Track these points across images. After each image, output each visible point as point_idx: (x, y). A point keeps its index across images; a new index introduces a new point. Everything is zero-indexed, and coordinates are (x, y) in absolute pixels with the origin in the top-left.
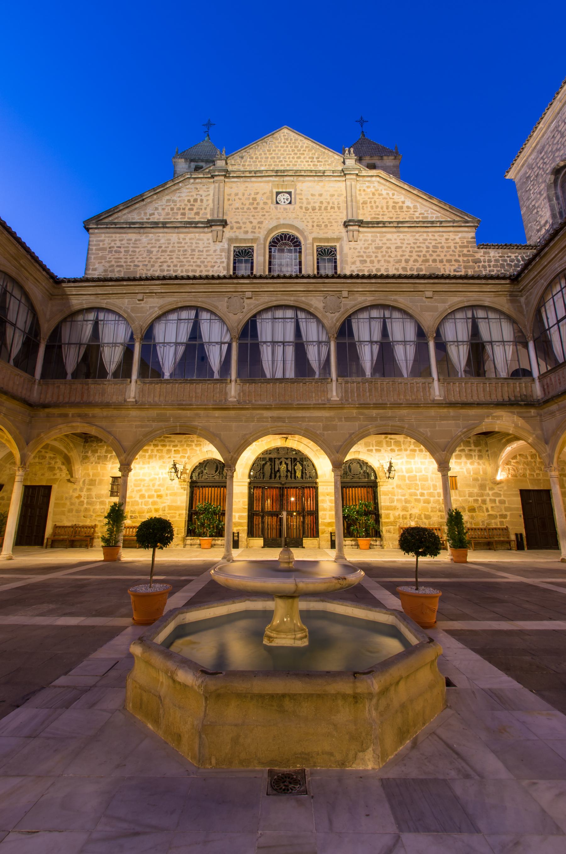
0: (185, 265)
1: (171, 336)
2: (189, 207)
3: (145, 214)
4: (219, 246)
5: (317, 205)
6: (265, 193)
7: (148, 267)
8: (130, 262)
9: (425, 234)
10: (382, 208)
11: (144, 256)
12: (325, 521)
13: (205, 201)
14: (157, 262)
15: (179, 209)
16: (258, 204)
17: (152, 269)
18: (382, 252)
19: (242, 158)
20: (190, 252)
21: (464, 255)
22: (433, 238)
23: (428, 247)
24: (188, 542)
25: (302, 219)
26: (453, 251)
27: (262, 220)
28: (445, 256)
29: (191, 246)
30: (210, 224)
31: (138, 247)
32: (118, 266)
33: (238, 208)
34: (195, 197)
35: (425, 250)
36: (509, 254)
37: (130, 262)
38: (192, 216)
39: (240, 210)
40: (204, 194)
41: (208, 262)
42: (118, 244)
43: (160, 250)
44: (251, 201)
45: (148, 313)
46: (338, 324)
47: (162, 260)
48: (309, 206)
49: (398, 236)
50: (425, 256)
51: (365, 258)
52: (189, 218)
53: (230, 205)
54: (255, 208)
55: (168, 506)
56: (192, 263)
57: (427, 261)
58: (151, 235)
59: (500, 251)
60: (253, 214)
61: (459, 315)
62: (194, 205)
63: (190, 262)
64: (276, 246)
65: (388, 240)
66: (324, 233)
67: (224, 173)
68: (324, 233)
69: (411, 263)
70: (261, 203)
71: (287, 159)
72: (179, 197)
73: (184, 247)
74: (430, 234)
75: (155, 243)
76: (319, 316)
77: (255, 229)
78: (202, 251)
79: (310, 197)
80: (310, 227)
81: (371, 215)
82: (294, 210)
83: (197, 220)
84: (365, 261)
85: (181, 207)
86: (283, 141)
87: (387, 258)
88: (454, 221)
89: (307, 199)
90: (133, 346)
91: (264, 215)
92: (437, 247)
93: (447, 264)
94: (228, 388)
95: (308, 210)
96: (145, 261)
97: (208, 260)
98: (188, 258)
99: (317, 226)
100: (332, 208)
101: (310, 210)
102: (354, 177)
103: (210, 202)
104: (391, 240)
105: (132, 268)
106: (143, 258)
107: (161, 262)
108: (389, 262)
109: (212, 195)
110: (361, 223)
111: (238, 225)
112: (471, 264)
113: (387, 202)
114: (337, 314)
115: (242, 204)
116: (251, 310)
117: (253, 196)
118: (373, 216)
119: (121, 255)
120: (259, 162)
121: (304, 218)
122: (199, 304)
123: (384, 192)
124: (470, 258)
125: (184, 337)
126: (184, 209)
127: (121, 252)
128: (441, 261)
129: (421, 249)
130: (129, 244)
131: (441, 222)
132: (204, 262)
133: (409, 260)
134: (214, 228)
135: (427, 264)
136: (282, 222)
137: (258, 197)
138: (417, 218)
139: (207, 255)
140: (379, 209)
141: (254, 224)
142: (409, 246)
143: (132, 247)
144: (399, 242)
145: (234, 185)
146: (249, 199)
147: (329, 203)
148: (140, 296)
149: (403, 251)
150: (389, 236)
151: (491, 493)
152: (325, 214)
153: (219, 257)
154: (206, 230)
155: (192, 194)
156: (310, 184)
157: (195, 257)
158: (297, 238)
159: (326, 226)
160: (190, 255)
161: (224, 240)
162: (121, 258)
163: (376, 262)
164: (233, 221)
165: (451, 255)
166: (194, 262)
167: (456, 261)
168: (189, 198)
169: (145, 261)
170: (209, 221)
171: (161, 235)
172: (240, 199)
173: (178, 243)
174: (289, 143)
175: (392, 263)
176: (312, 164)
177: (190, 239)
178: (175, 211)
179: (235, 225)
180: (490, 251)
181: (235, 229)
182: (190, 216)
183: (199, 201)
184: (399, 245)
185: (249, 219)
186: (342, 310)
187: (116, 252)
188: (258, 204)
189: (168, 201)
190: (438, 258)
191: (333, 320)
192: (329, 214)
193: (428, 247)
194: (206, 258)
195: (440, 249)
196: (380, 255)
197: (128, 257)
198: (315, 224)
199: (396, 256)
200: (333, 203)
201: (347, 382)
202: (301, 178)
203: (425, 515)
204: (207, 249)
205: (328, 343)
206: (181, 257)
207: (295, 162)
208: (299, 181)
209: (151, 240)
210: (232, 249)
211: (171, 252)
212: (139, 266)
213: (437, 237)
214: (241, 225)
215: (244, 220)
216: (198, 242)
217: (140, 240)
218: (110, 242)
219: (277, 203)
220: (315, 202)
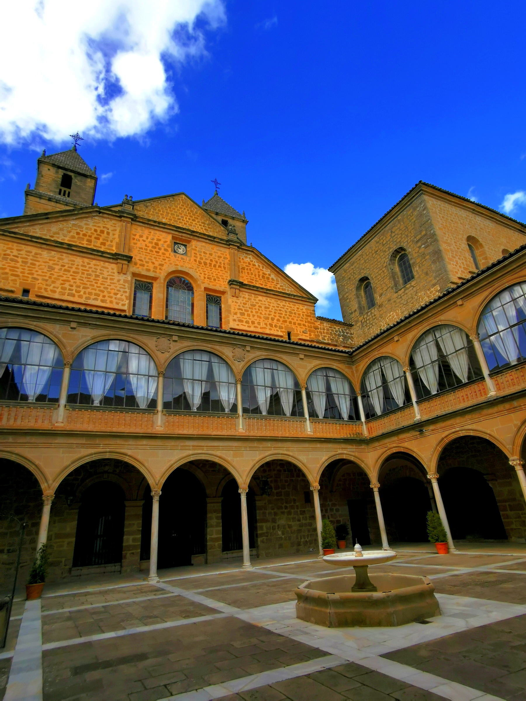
0: (89, 288)
2: (95, 236)
3: (49, 230)
4: (122, 277)
5: (208, 262)
6: (166, 242)
7: (49, 283)
8: (28, 274)
9: (284, 302)
10: (255, 276)
11: (45, 271)
12: (212, 537)
13: (111, 234)
14: (59, 279)
15: (85, 235)
16: (160, 249)
17: (53, 285)
18: (255, 309)
19: (147, 207)
20: (93, 277)
21: (309, 322)
22: (289, 305)
23: (286, 312)
24: (73, 573)
25: (196, 269)
26: (302, 318)
27: (162, 263)
28: (297, 320)
29: (96, 272)
30: (116, 257)
31: (39, 261)
32: (12, 275)
33: (142, 248)
34: (102, 229)
35: (284, 313)
36: (335, 327)
37: (28, 274)
38: (98, 244)
39: (144, 250)
40: (111, 228)
41: (111, 289)
42: (15, 253)
43: (63, 268)
44: (154, 245)
45: (80, 341)
46: (243, 370)
47: (64, 278)
48: (202, 261)
49: (267, 299)
50: (284, 317)
51: (244, 311)
52: (94, 246)
53: (135, 244)
54: (157, 252)
56: (95, 287)
57: (285, 321)
58: (53, 253)
59: (330, 323)
60: (155, 256)
61: (319, 373)
62: (101, 236)
63: (93, 286)
64: (172, 287)
65: (259, 300)
66: (213, 285)
67: (132, 217)
68: (213, 285)
69: (275, 321)
70: (163, 248)
71: (184, 219)
72: (86, 224)
73: (88, 271)
74: (287, 303)
75: (58, 261)
77: (156, 269)
78: (107, 278)
79: (202, 254)
80: (203, 278)
81: (248, 279)
82: (190, 260)
83: (102, 250)
84: (244, 314)
85: (88, 234)
86: (181, 203)
87: (259, 314)
88: (303, 297)
89: (200, 255)
91: (165, 260)
92: (292, 313)
93: (299, 327)
94: (154, 418)
95: (201, 264)
96: (45, 276)
97: (111, 287)
98: (92, 282)
99: (208, 278)
100: (220, 267)
101: (203, 264)
102: (236, 248)
103: (117, 236)
104: (261, 301)
105: (30, 279)
106: (43, 272)
107: (62, 280)
108: (260, 318)
109: (118, 231)
110: (242, 285)
111: (141, 263)
112: (313, 329)
113: (259, 272)
114: (243, 363)
115: (146, 245)
117: (155, 241)
118: (249, 280)
119: (18, 265)
120: (161, 214)
121: (198, 269)
122: (130, 339)
123: (257, 264)
124: (312, 325)
126: (90, 236)
127: (18, 262)
128: (295, 324)
129: (282, 312)
130: (29, 256)
131: (295, 296)
132: (107, 288)
133: (274, 319)
134: (119, 261)
135: (286, 324)
136: (180, 268)
137: (160, 243)
138: (279, 288)
139: (111, 283)
140: (253, 276)
141: (155, 265)
142: (274, 309)
143: (31, 259)
144: (267, 303)
145: (139, 229)
146: (151, 243)
147: (217, 262)
148: (73, 325)
149: (270, 311)
150: (260, 298)
151: (330, 503)
152: (213, 270)
153: (122, 286)
154: (111, 260)
155: (99, 225)
156: (204, 244)
157: (99, 282)
158: (190, 283)
159: (215, 280)
160: (94, 279)
161: (128, 273)
162: (17, 268)
163: (251, 315)
164: (137, 258)
165: (300, 320)
166: (97, 287)
167: (304, 325)
168: (95, 228)
169: (45, 276)
170: (116, 254)
171: (64, 255)
172: (144, 241)
173: (82, 266)
174: (186, 207)
175: (263, 319)
176: (204, 228)
177: (95, 265)
178: (81, 236)
179: (139, 262)
180: (324, 322)
181: (138, 266)
182: (96, 245)
183: (105, 232)
184: (268, 306)
185: (151, 260)
186: (246, 360)
187: (12, 260)
188: (160, 249)
189: (74, 225)
190: (293, 321)
191: (239, 367)
192: (217, 271)
193: (286, 312)
194: (110, 286)
195: (294, 315)
196: (254, 311)
197: (26, 268)
198: (206, 276)
199: (265, 314)
200: (220, 263)
201: (249, 418)
202: (196, 238)
203: (288, 524)
204: (111, 277)
205: (236, 384)
206: (84, 279)
207: (191, 222)
208: (195, 240)
209: (54, 257)
210: (134, 281)
211: (74, 272)
212: (38, 280)
213: (291, 306)
214: (144, 263)
215: (147, 260)
216: (102, 269)
217: (41, 254)
218: (5, 249)
219: (175, 252)
220: (206, 259)
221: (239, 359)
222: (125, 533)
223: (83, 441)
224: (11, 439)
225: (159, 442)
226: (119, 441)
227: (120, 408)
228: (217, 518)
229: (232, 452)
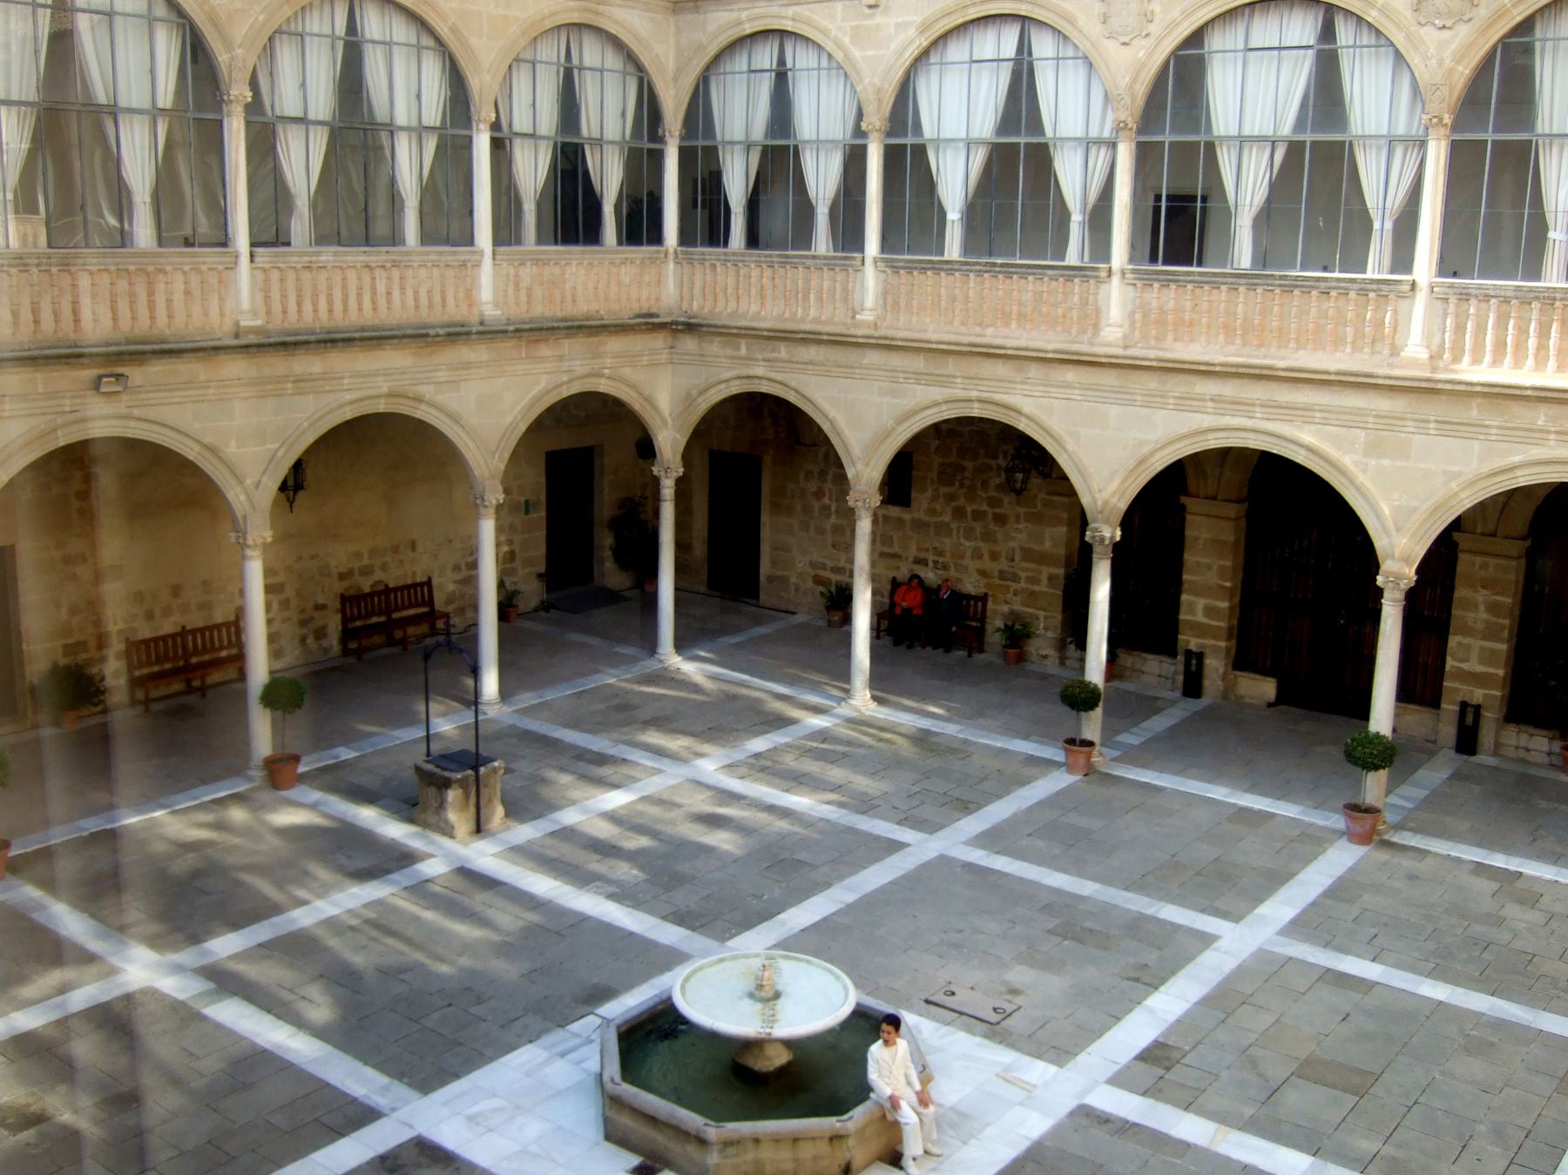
1: (960, 115)
12: (1465, 666)
45: (893, 46)
55: (1022, 549)
76: (1398, 39)
90: (864, 148)
94: (1100, 296)
116: (1174, 24)
125: (985, 125)
221: (1439, 14)
222: (1185, 586)
223: (918, 363)
224: (783, 351)
225: (1109, 378)
226: (1001, 369)
227: (1002, 265)
228: (1493, 608)
229: (1362, 434)
